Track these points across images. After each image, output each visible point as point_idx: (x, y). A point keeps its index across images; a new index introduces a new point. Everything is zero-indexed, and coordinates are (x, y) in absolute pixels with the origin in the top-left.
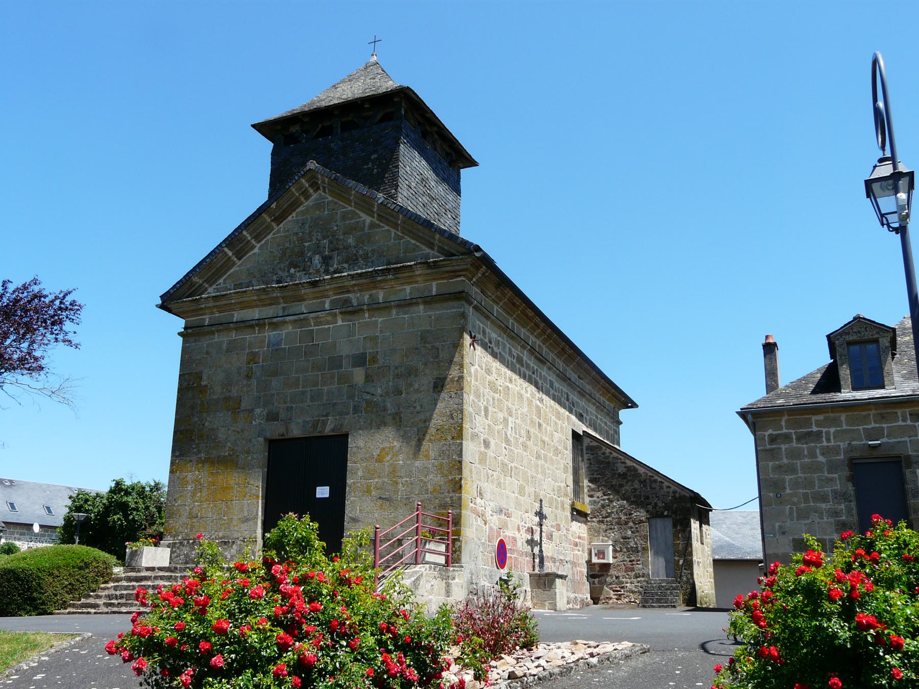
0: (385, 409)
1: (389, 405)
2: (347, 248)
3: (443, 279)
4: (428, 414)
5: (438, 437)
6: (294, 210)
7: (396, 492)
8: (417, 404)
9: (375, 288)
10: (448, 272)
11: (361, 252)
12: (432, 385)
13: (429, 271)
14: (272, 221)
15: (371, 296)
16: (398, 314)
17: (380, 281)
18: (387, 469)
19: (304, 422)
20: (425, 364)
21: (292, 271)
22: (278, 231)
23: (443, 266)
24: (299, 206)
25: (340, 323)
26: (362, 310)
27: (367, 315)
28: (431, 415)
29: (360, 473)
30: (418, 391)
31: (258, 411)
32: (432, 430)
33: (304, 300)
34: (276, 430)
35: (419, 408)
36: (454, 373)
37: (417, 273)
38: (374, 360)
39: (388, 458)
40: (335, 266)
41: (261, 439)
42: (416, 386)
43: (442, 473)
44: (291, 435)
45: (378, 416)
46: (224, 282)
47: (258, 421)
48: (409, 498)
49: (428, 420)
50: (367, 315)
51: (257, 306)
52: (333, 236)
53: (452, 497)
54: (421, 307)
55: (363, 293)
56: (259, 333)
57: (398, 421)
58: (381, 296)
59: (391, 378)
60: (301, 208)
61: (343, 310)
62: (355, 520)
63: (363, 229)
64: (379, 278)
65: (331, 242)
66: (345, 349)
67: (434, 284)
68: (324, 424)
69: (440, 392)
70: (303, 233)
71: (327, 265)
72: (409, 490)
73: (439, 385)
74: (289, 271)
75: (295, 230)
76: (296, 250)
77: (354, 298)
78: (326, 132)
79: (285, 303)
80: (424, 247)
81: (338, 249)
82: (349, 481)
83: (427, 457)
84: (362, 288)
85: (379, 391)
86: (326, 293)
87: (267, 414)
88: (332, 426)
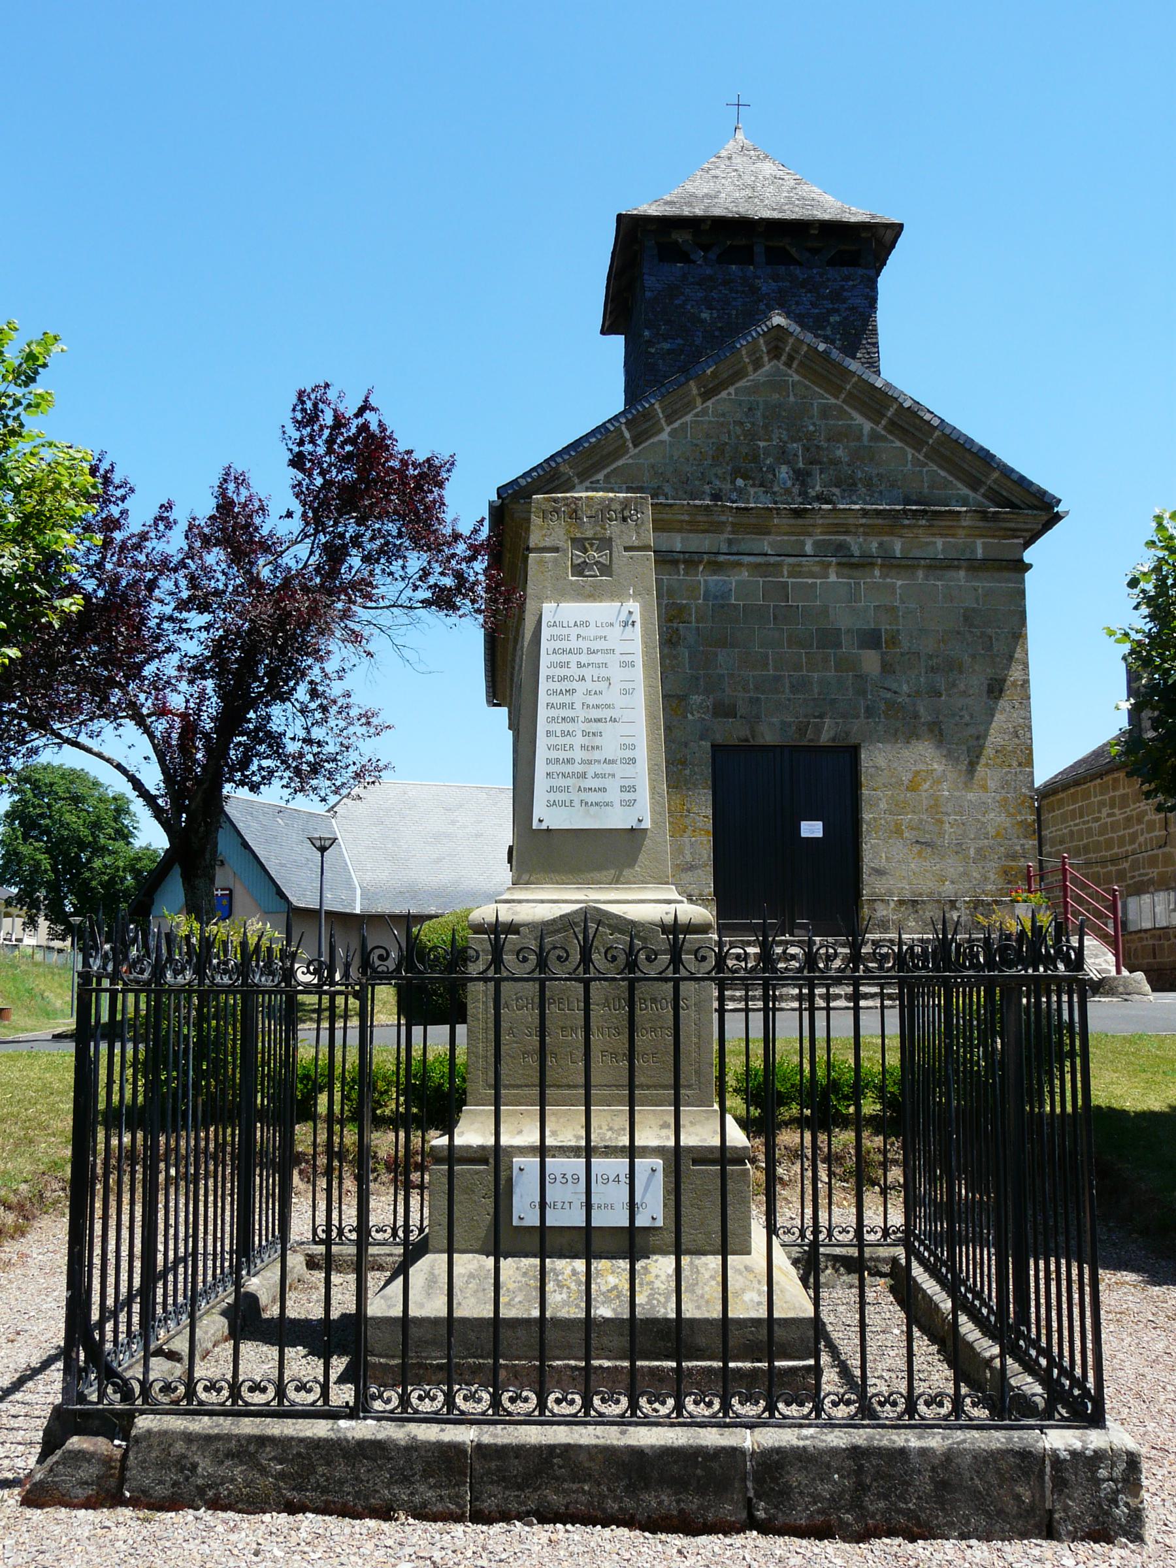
0: (916, 716)
1: (922, 711)
2: (835, 462)
3: (993, 537)
4: (982, 728)
5: (999, 761)
6: (732, 384)
7: (941, 834)
8: (964, 713)
9: (892, 534)
10: (1005, 529)
11: (860, 475)
12: (985, 688)
13: (981, 524)
14: (700, 395)
15: (881, 544)
16: (926, 578)
17: (909, 526)
18: (925, 802)
19: (783, 723)
20: (973, 657)
21: (740, 482)
22: (704, 412)
23: (1004, 520)
24: (741, 379)
25: (833, 578)
26: (872, 565)
27: (877, 573)
28: (987, 730)
29: (883, 805)
30: (964, 693)
31: (696, 699)
32: (989, 751)
33: (769, 533)
34: (732, 732)
35: (967, 718)
36: (1015, 674)
37: (964, 524)
38: (894, 640)
39: (926, 786)
40: (818, 488)
41: (706, 745)
42: (962, 687)
43: (1007, 811)
44: (760, 741)
45: (905, 725)
46: (607, 476)
47: (697, 716)
48: (960, 844)
49: (981, 737)
50: (877, 573)
51: (680, 531)
52: (809, 440)
53: (1022, 845)
54: (962, 573)
55: (870, 538)
56: (686, 574)
57: (937, 732)
58: (898, 547)
59: (923, 671)
60: (742, 383)
61: (844, 560)
62: (879, 872)
63: (859, 439)
64: (906, 522)
65: (806, 449)
66: (843, 620)
67: (979, 542)
68: (818, 729)
69: (998, 698)
70: (753, 424)
71: (804, 484)
72: (960, 832)
73: (996, 689)
74: (733, 482)
75: (738, 416)
76: (744, 450)
77: (855, 544)
78: (744, 256)
79: (733, 532)
80: (960, 485)
81: (820, 463)
82: (867, 816)
83: (984, 788)
84: (869, 531)
85: (905, 688)
86: (811, 529)
87: (715, 706)
88: (832, 734)
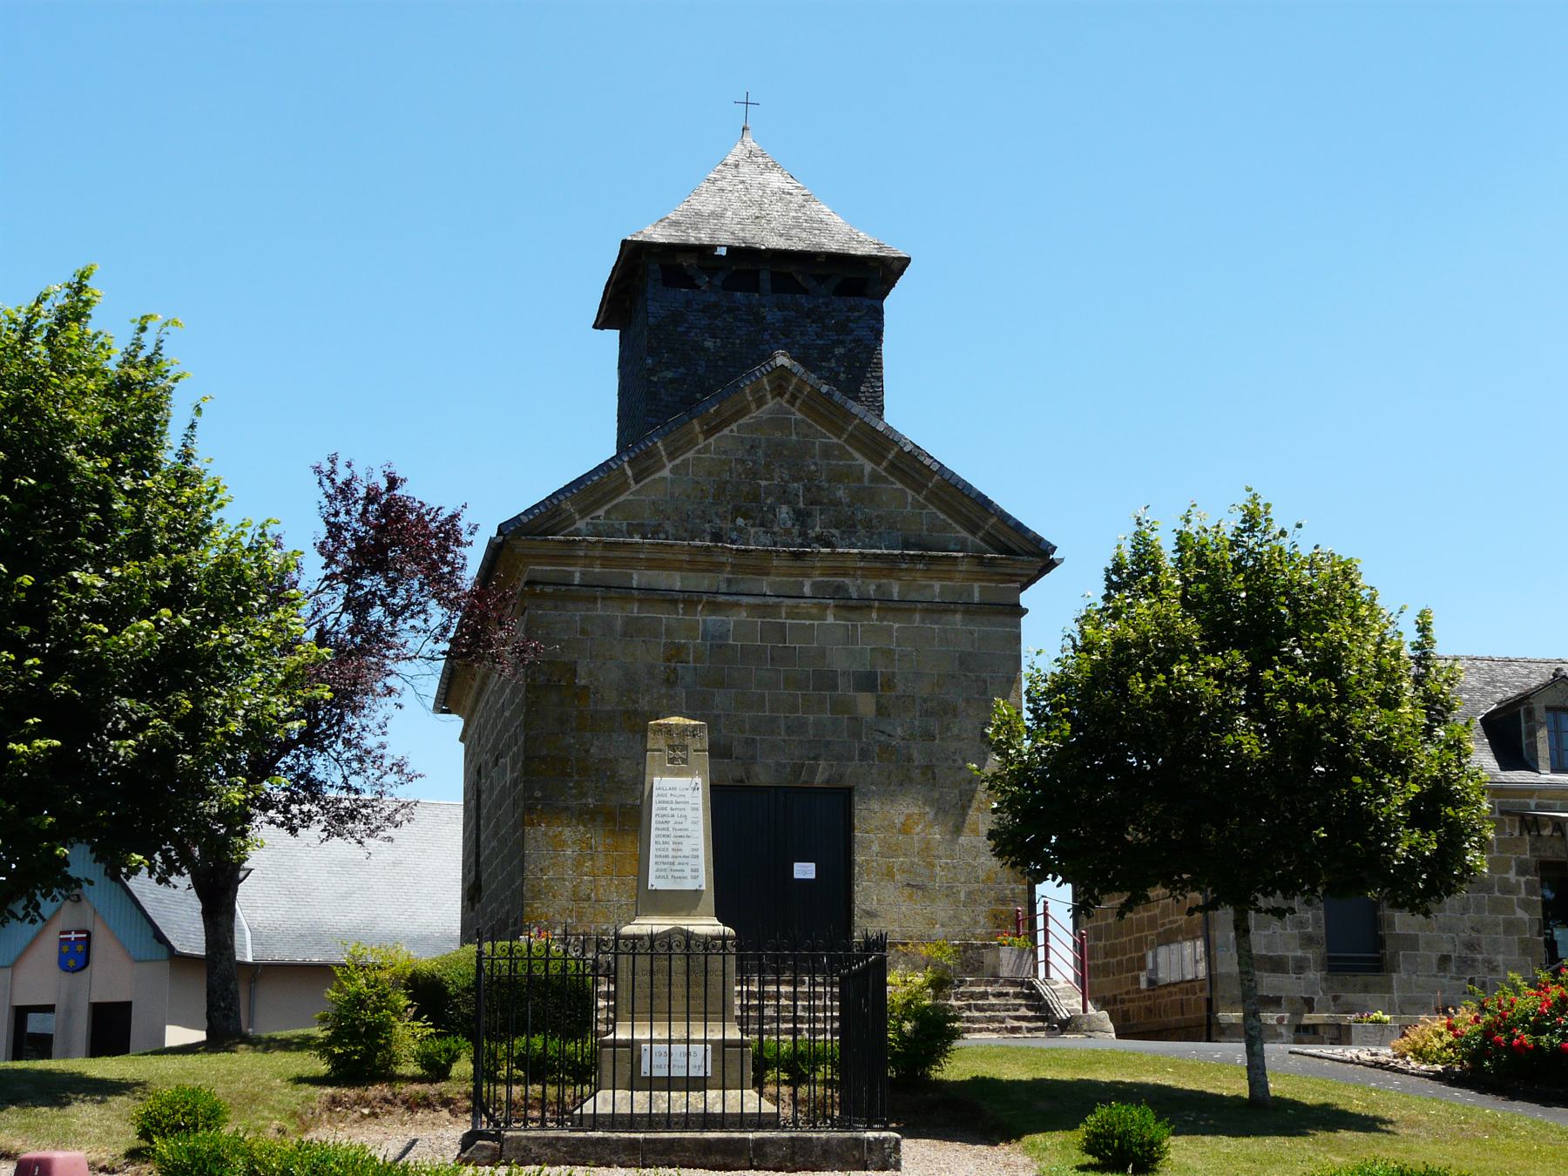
0: (909, 759)
1: (915, 754)
2: (836, 503)
7: (933, 877)
9: (889, 576)
11: (860, 516)
13: (979, 569)
15: (879, 586)
16: (923, 621)
20: (968, 701)
21: (740, 521)
22: (706, 449)
23: (1000, 565)
25: (830, 620)
26: (870, 607)
27: (874, 615)
29: (876, 848)
30: (958, 738)
33: (768, 574)
38: (889, 683)
42: (956, 730)
46: (608, 513)
50: (874, 615)
51: (680, 569)
54: (958, 617)
56: (685, 613)
57: (930, 774)
58: (895, 591)
61: (842, 602)
62: (871, 914)
64: (904, 566)
65: (807, 489)
66: (840, 662)
68: (813, 771)
70: (754, 462)
71: (803, 524)
74: (733, 521)
75: (739, 455)
76: (745, 489)
77: (853, 586)
82: (859, 858)
83: (975, 832)
84: (868, 573)
85: (899, 730)
